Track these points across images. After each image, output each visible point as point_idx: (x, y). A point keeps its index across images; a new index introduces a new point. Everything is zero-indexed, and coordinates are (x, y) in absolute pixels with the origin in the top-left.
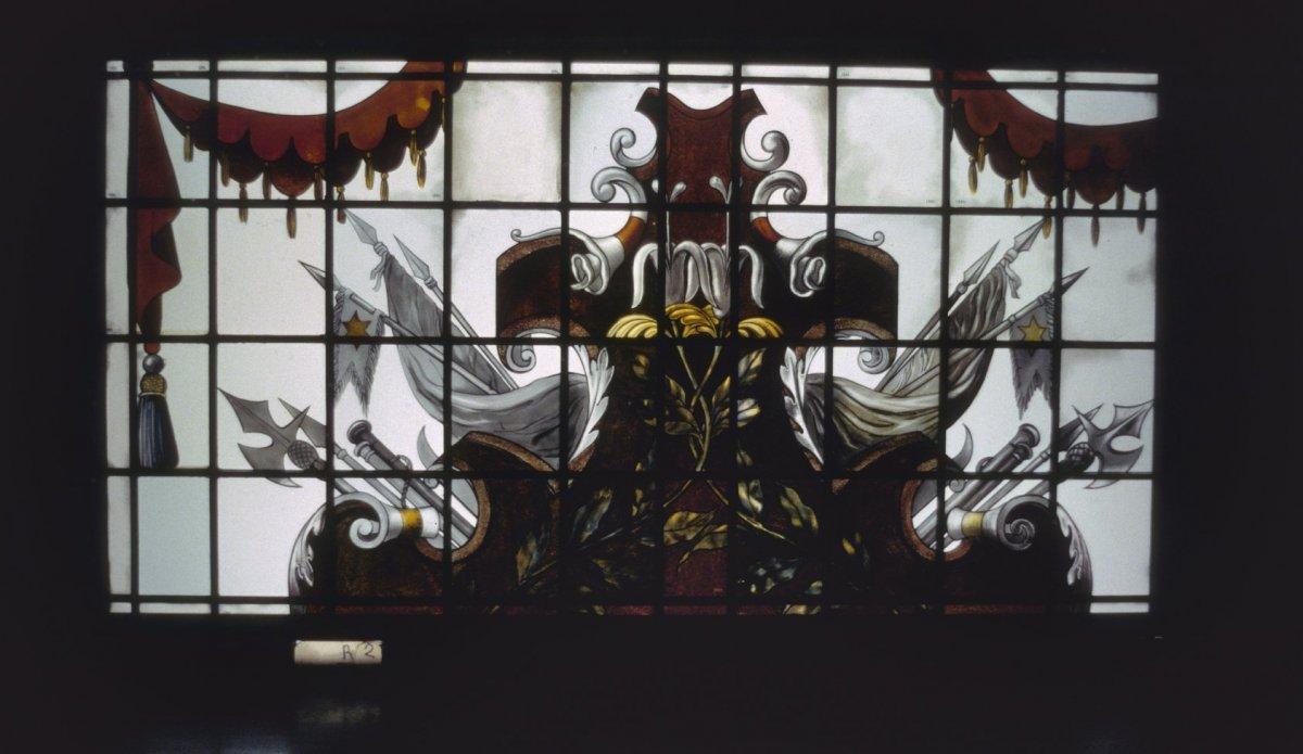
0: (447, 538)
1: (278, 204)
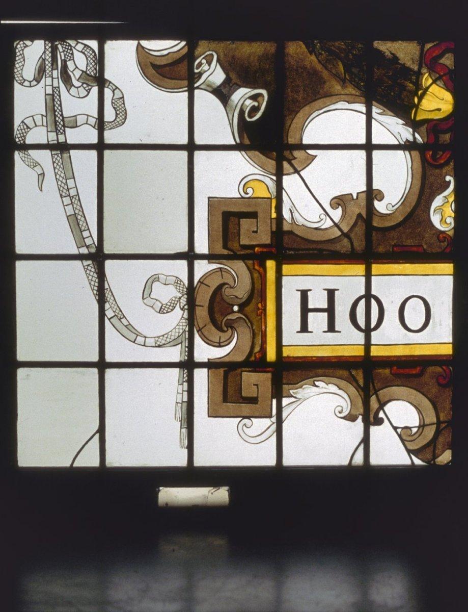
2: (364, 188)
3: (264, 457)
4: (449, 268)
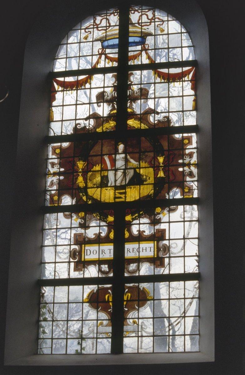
0: (89, 127)
1: (70, 90)
2: (99, 232)
3: (82, 276)
4: (112, 244)
